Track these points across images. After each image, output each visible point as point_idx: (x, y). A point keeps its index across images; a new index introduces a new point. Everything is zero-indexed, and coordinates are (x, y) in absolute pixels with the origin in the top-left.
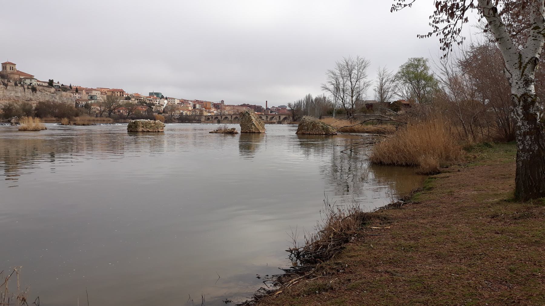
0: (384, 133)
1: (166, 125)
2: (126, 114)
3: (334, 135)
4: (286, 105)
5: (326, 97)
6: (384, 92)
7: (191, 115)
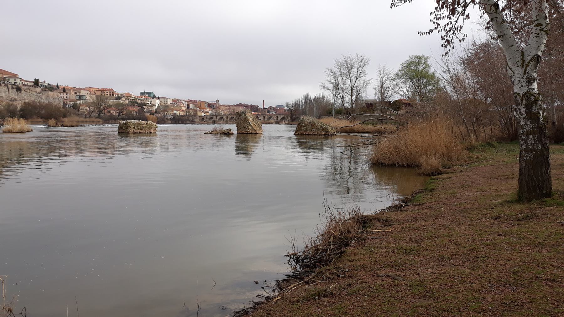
0: (384, 133)
1: (159, 125)
2: (116, 115)
3: (334, 135)
4: (284, 104)
5: (324, 97)
6: (385, 91)
7: (184, 115)
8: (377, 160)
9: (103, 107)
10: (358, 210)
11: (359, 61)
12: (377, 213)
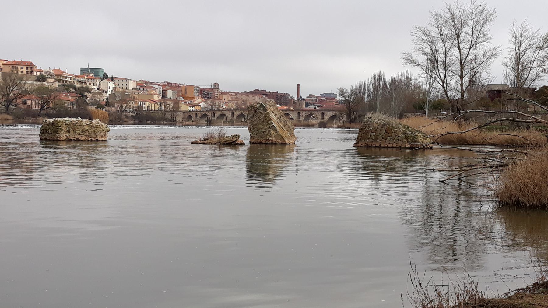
0: (523, 146)
1: (111, 127)
2: (37, 108)
3: (427, 148)
4: (336, 91)
5: (411, 78)
6: (524, 69)
7: (157, 109)
8: (509, 196)
9: (14, 94)
10: (475, 290)
11: (476, 14)
12: (509, 295)
